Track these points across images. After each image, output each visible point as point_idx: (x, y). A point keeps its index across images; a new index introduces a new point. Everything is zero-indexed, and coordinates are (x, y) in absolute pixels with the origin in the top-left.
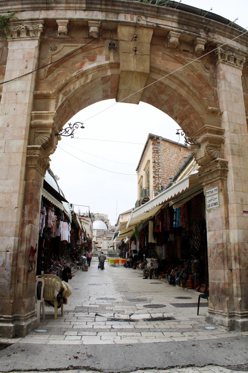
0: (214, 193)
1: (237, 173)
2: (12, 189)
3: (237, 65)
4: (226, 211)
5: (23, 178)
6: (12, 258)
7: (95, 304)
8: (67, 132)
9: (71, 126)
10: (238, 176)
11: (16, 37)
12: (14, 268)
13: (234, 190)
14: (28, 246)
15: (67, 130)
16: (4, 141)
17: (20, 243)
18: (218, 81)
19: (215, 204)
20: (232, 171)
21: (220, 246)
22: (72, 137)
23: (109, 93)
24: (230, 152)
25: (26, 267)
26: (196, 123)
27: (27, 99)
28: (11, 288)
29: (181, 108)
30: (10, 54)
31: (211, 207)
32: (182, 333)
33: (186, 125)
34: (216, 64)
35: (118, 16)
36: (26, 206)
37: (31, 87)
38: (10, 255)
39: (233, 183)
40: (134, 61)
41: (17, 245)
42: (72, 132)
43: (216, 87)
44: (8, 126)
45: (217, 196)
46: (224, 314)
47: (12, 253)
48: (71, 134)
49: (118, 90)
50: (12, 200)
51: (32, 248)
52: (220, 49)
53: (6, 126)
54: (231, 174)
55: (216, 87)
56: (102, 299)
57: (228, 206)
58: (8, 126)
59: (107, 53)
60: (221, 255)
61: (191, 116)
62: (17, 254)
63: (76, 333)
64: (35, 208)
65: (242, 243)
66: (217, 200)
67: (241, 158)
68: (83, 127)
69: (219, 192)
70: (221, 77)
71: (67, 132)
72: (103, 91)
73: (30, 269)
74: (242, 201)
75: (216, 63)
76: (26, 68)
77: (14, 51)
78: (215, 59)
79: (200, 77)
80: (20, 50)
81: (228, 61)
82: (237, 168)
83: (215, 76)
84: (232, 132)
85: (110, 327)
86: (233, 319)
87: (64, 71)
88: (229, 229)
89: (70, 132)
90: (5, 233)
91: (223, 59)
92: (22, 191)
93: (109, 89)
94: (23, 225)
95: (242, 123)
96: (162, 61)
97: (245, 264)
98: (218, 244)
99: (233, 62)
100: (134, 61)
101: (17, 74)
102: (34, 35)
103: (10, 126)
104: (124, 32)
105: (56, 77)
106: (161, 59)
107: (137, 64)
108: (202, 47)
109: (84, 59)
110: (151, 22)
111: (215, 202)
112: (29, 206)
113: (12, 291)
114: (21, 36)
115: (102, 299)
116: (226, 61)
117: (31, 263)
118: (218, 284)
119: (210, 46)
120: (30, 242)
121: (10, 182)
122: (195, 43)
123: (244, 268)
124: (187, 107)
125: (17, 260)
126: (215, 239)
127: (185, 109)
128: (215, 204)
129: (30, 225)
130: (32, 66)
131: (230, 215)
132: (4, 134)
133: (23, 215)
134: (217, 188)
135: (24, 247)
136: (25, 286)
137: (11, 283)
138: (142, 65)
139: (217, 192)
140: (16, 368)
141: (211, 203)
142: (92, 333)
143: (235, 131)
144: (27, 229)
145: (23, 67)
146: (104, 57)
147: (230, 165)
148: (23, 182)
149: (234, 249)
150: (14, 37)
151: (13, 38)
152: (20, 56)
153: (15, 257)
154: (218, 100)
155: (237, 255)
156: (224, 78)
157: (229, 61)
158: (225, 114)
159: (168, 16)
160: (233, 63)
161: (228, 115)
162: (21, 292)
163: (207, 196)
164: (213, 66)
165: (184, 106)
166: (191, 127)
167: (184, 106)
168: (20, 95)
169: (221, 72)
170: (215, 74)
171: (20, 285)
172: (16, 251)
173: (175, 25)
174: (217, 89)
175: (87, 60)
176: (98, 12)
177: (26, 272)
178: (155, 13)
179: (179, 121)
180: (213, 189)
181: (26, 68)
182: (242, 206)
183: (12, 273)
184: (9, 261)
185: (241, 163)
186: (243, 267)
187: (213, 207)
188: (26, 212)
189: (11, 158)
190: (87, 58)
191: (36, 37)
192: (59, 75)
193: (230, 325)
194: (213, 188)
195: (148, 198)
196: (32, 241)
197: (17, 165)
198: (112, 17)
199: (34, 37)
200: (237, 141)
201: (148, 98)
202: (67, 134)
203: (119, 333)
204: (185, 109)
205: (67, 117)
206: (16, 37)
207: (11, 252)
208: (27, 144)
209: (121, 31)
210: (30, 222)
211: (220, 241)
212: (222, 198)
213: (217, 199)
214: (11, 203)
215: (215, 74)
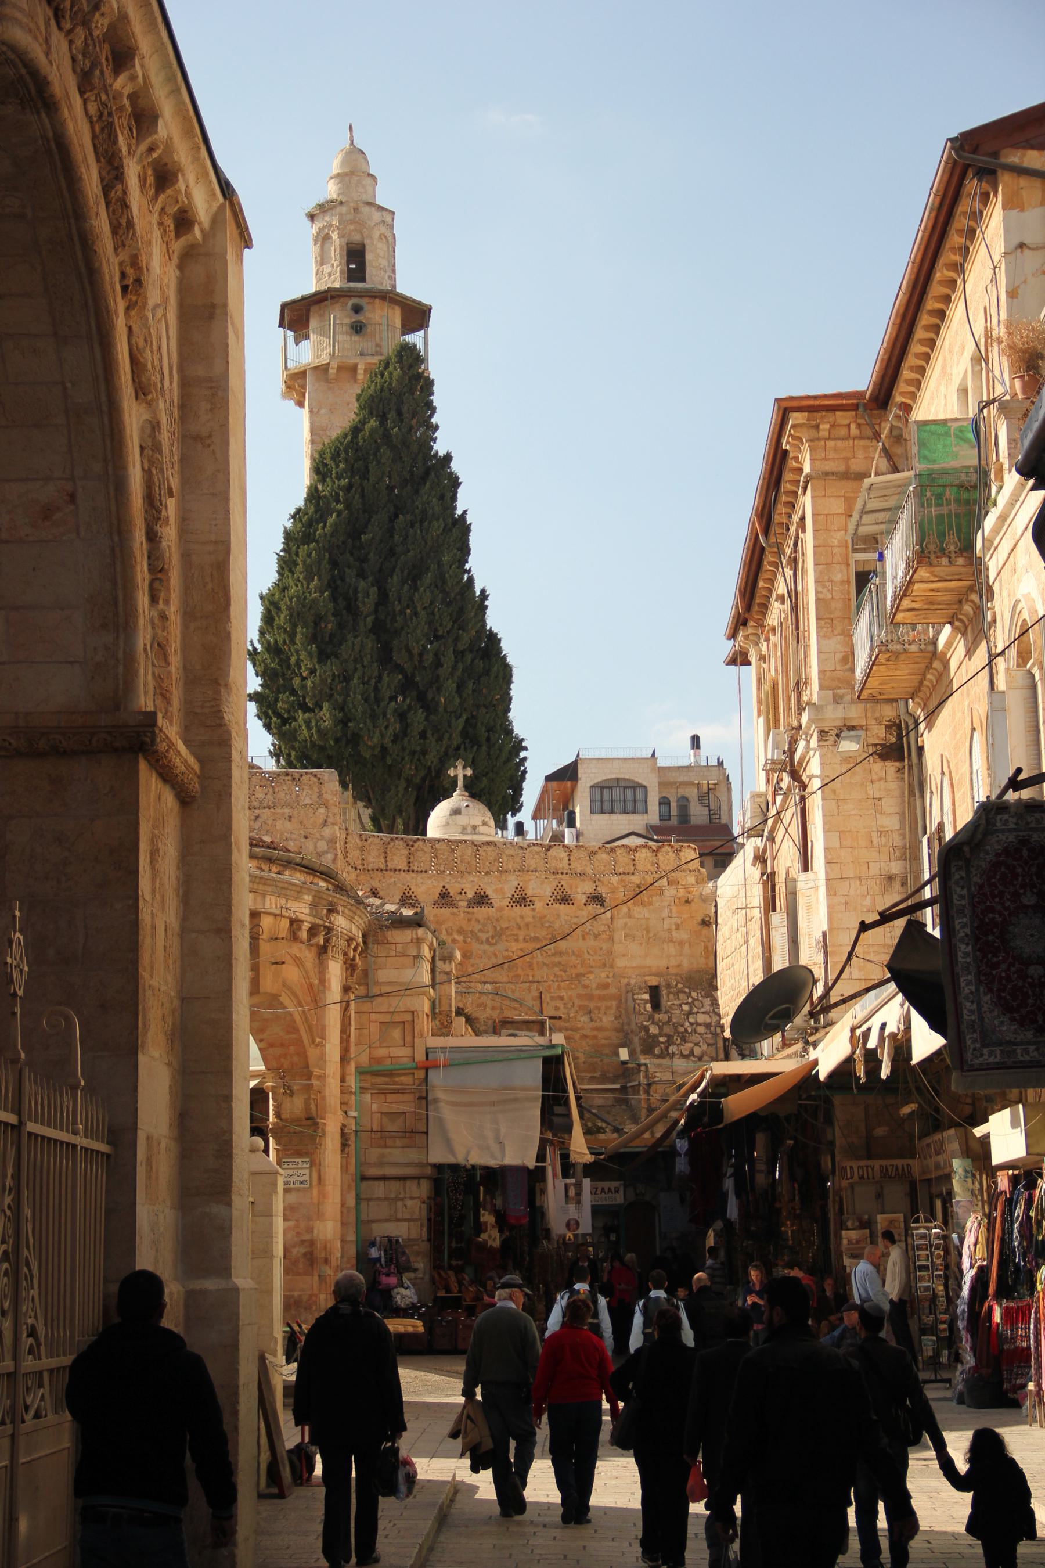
0: (300, 1166)
26: (296, 1059)
31: (292, 1186)
45: (307, 1172)
66: (306, 1178)
79: (311, 986)
98: (303, 1242)
118: (300, 1296)
124: (294, 1036)
127: (287, 1037)
128: (301, 1183)
141: (292, 1180)
149: (325, 1248)
159: (306, 897)
165: (288, 1033)
167: (288, 1033)
173: (307, 911)
178: (295, 894)
179: (262, 1045)
180: (300, 1160)
187: (297, 1186)
198: (259, 907)
211: (307, 1237)
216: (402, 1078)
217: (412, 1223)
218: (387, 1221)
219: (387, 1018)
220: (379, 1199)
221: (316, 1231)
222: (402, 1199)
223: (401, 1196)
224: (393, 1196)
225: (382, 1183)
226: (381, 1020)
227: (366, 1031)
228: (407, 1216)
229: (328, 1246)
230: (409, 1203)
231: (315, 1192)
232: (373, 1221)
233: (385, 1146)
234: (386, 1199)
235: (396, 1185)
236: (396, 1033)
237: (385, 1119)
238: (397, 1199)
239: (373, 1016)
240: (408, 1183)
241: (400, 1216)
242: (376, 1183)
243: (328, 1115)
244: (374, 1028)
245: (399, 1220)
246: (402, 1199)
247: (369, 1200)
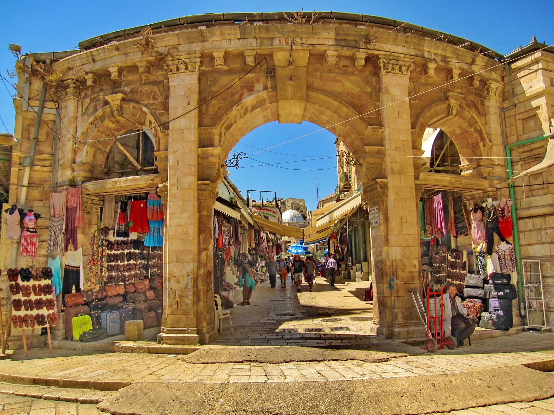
0: (375, 212)
1: (397, 193)
2: (188, 221)
3: (402, 73)
4: (386, 230)
5: (196, 212)
6: (193, 281)
7: (273, 320)
8: (232, 163)
9: (236, 157)
10: (398, 195)
11: (175, 72)
12: (195, 289)
13: (392, 209)
14: (205, 270)
15: (232, 161)
16: (176, 178)
17: (199, 268)
18: (381, 94)
19: (377, 222)
20: (392, 190)
21: (380, 262)
22: (237, 168)
23: (270, 117)
24: (390, 171)
25: (205, 288)
27: (193, 137)
28: (194, 306)
29: (343, 128)
30: (171, 90)
31: (374, 225)
32: (342, 340)
33: (349, 143)
34: (380, 76)
35: (273, 42)
36: (201, 236)
37: (195, 124)
38: (191, 278)
39: (392, 202)
40: (291, 88)
41: (196, 270)
42: (237, 163)
43: (378, 101)
44: (178, 164)
45: (377, 215)
46: (384, 324)
47: (192, 277)
48: (236, 165)
49: (278, 115)
50: (189, 232)
51: (209, 271)
52: (383, 60)
53: (176, 163)
54: (391, 194)
55: (378, 101)
56: (280, 315)
57: (387, 225)
58: (178, 164)
59: (265, 81)
60: (381, 271)
61: (352, 135)
62: (197, 277)
63: (250, 341)
64: (209, 236)
65: (400, 260)
66: (377, 219)
67: (402, 176)
68: (246, 157)
69: (379, 211)
70: (384, 91)
71: (232, 163)
72: (264, 117)
73: (208, 289)
74: (401, 219)
75: (379, 74)
76: (189, 104)
77: (175, 87)
78: (379, 70)
80: (181, 86)
81: (392, 72)
82: (397, 188)
83: (378, 89)
84: (393, 150)
85: (281, 337)
86: (390, 329)
87: (224, 104)
88: (388, 246)
89: (235, 163)
90: (186, 260)
91: (386, 71)
92: (196, 222)
93: (270, 115)
94: (200, 252)
95: (405, 139)
96: (320, 82)
97: (403, 279)
98: (379, 261)
99: (398, 72)
100: (291, 88)
101: (180, 111)
102: (192, 69)
103: (180, 164)
104: (280, 58)
105: (218, 110)
106: (319, 80)
107: (294, 92)
108: (363, 62)
109: (242, 89)
110: (306, 43)
111: (376, 220)
112: (203, 236)
113: (195, 308)
114: (180, 71)
115: (280, 315)
116: (390, 72)
117: (209, 284)
119: (371, 60)
120: (206, 266)
121: (186, 215)
122: (355, 57)
123: (402, 283)
125: (197, 283)
126: (377, 256)
127: (346, 129)
128: (377, 222)
129: (206, 251)
130: (194, 103)
131: (389, 233)
132: (175, 172)
133: (199, 243)
134: (377, 207)
135: (202, 271)
136: (205, 303)
137: (194, 302)
138: (299, 92)
139: (377, 211)
140: (205, 361)
141: (373, 221)
142: (264, 341)
143: (397, 149)
144: (204, 254)
145: (185, 104)
146: (262, 85)
147: (389, 185)
148: (197, 215)
150: (173, 72)
151: (173, 74)
152: (182, 93)
153: (196, 280)
154: (380, 116)
155: (395, 271)
156: (387, 92)
157: (393, 71)
158: (387, 131)
160: (399, 72)
161: (389, 132)
162: (203, 309)
163: (371, 213)
164: (376, 78)
166: (354, 145)
168: (185, 133)
169: (384, 85)
170: (378, 86)
171: (201, 304)
172: (196, 275)
173: (332, 42)
174: (380, 104)
175: (245, 90)
176: (253, 40)
177: (205, 292)
180: (375, 208)
181: (189, 104)
182: (401, 224)
183: (194, 293)
184: (191, 284)
185: (402, 181)
186: (401, 282)
188: (201, 241)
189: (184, 194)
190: (245, 88)
191: (194, 71)
192: (220, 108)
193: (387, 334)
194: (375, 206)
195: (350, 184)
196: (208, 265)
197: (190, 200)
199: (192, 71)
200: (398, 159)
201: (309, 118)
202: (232, 165)
203: (286, 341)
204: (346, 129)
205: (231, 145)
206: (175, 72)
207: (191, 276)
208: (197, 180)
209: (276, 57)
210: (206, 249)
212: (382, 217)
213: (378, 218)
214: (188, 234)
215: (378, 86)
216: (538, 150)
217: (551, 245)
218: (536, 244)
219: (526, 115)
220: (531, 230)
221: (384, 254)
222: (545, 229)
223: (544, 227)
224: (538, 227)
225: (531, 220)
226: (522, 118)
227: (514, 127)
228: (549, 240)
229: (394, 264)
230: (549, 231)
231: (382, 228)
232: (529, 245)
233: (533, 196)
234: (535, 230)
235: (538, 220)
236: (532, 123)
237: (531, 179)
238: (541, 229)
239: (517, 117)
240: (547, 218)
241: (544, 240)
242: (528, 220)
243: (390, 176)
244: (519, 124)
245: (543, 243)
246: (545, 229)
247: (525, 231)
